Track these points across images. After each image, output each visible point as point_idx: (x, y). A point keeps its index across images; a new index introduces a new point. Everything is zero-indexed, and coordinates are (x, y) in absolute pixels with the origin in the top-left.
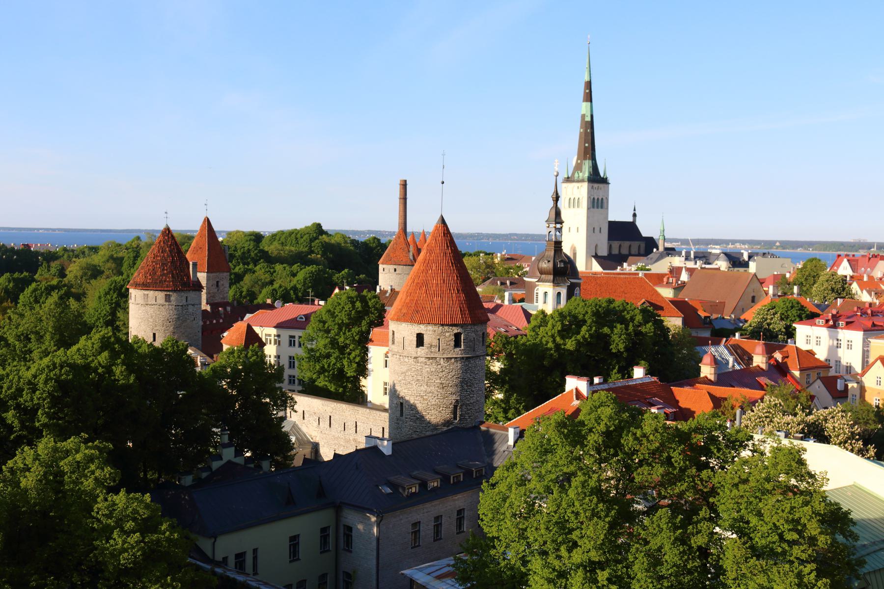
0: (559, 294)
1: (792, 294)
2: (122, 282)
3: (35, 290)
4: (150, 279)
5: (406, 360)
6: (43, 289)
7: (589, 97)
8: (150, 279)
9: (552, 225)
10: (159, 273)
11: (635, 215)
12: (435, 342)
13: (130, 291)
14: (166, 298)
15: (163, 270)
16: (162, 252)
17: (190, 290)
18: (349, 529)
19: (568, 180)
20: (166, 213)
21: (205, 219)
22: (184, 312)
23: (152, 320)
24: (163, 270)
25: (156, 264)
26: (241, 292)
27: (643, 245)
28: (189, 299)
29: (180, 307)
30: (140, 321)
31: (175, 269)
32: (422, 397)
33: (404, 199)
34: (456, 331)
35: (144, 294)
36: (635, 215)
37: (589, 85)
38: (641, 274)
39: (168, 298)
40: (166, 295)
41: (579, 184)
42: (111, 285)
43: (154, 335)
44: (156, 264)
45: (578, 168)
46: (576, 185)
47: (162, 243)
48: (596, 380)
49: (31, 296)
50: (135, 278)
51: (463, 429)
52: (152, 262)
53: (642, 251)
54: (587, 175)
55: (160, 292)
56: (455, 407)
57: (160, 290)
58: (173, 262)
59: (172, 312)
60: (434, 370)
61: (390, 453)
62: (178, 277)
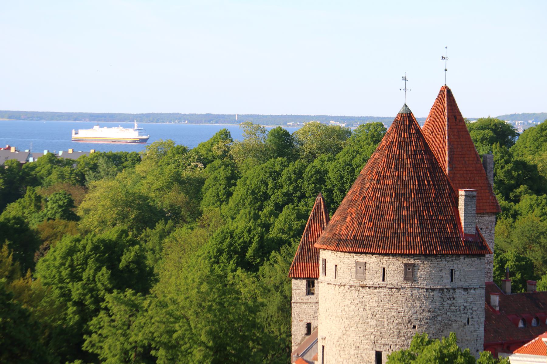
2: (246, 234)
3: (71, 252)
4: (370, 229)
6: (88, 248)
8: (370, 229)
10: (389, 216)
13: (324, 254)
14: (406, 274)
16: (397, 168)
17: (459, 256)
20: (405, 79)
21: (442, 92)
22: (446, 306)
23: (373, 323)
24: (400, 208)
25: (384, 195)
26: (503, 262)
28: (457, 274)
29: (436, 293)
30: (347, 322)
31: (427, 205)
35: (357, 263)
40: (406, 265)
42: (222, 242)
44: (384, 195)
47: (395, 148)
49: (63, 264)
50: (333, 226)
52: (375, 190)
55: (392, 259)
57: (394, 255)
58: (420, 191)
59: (418, 305)
62: (433, 225)
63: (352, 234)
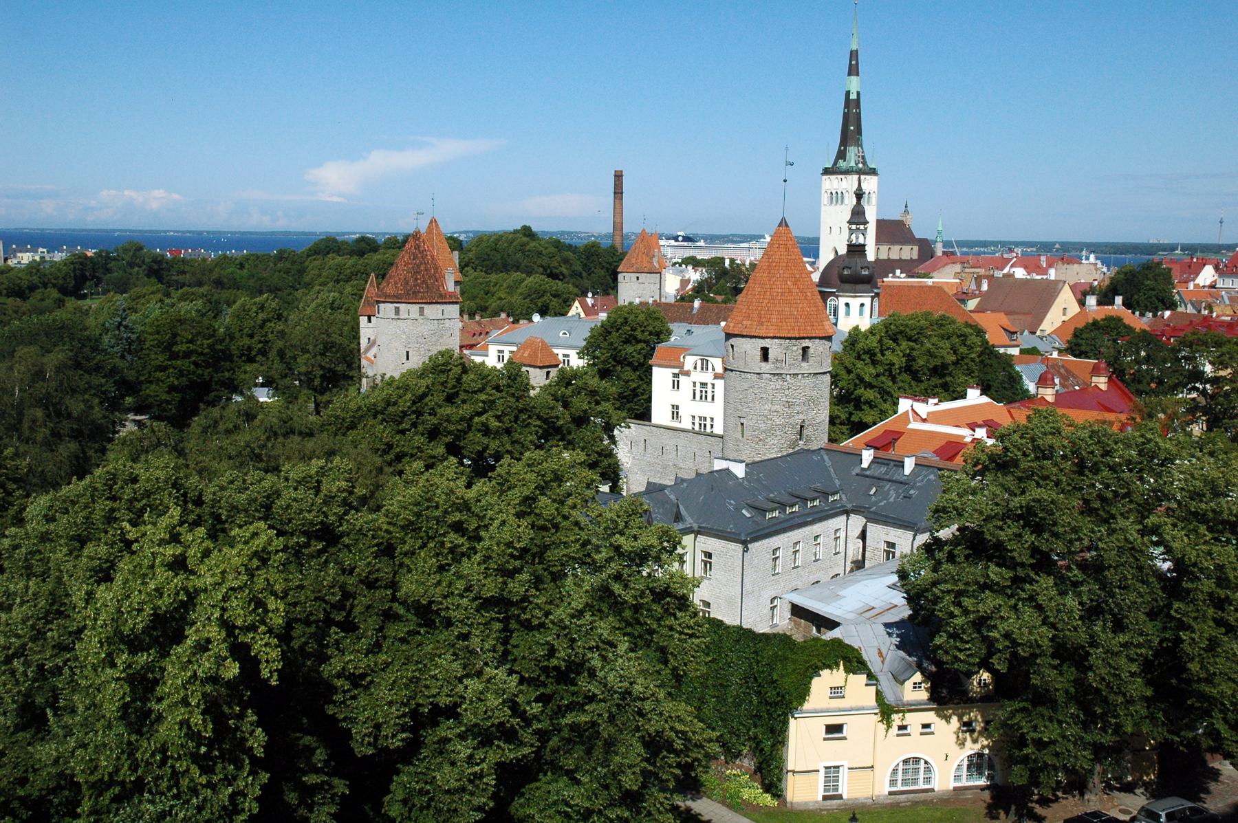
0: (862, 305)
1: (1112, 303)
5: (748, 376)
7: (853, 70)
9: (854, 227)
10: (411, 283)
11: (906, 212)
12: (781, 357)
15: (416, 279)
17: (446, 303)
18: (709, 555)
19: (827, 172)
24: (416, 279)
27: (916, 248)
32: (766, 416)
33: (618, 192)
34: (804, 345)
36: (906, 212)
37: (854, 55)
38: (929, 282)
39: (421, 311)
41: (842, 177)
43: (408, 352)
45: (841, 155)
46: (839, 177)
48: (931, 401)
51: (808, 450)
53: (915, 257)
54: (853, 164)
56: (802, 427)
60: (778, 387)
61: (743, 476)
63: (392, 292)
